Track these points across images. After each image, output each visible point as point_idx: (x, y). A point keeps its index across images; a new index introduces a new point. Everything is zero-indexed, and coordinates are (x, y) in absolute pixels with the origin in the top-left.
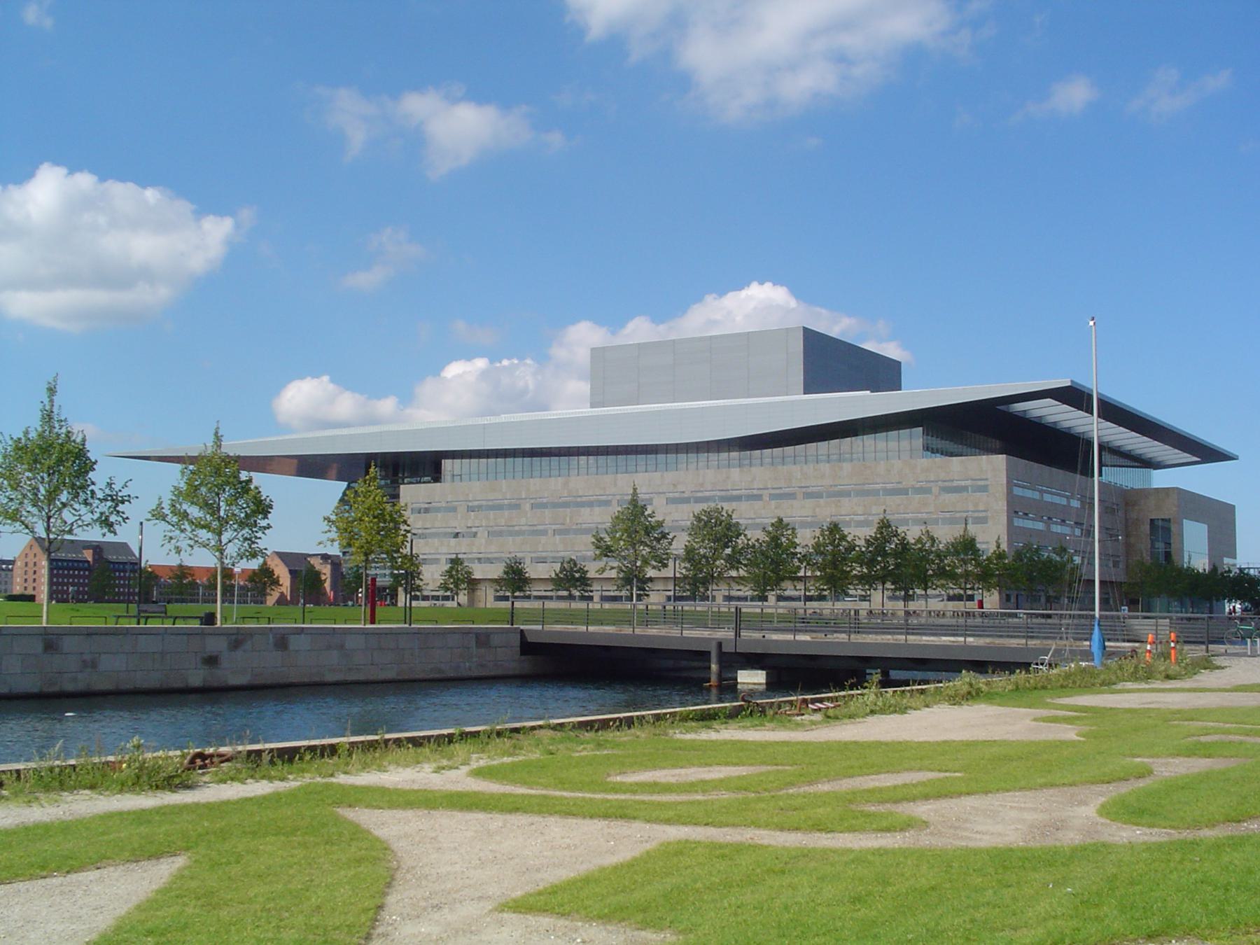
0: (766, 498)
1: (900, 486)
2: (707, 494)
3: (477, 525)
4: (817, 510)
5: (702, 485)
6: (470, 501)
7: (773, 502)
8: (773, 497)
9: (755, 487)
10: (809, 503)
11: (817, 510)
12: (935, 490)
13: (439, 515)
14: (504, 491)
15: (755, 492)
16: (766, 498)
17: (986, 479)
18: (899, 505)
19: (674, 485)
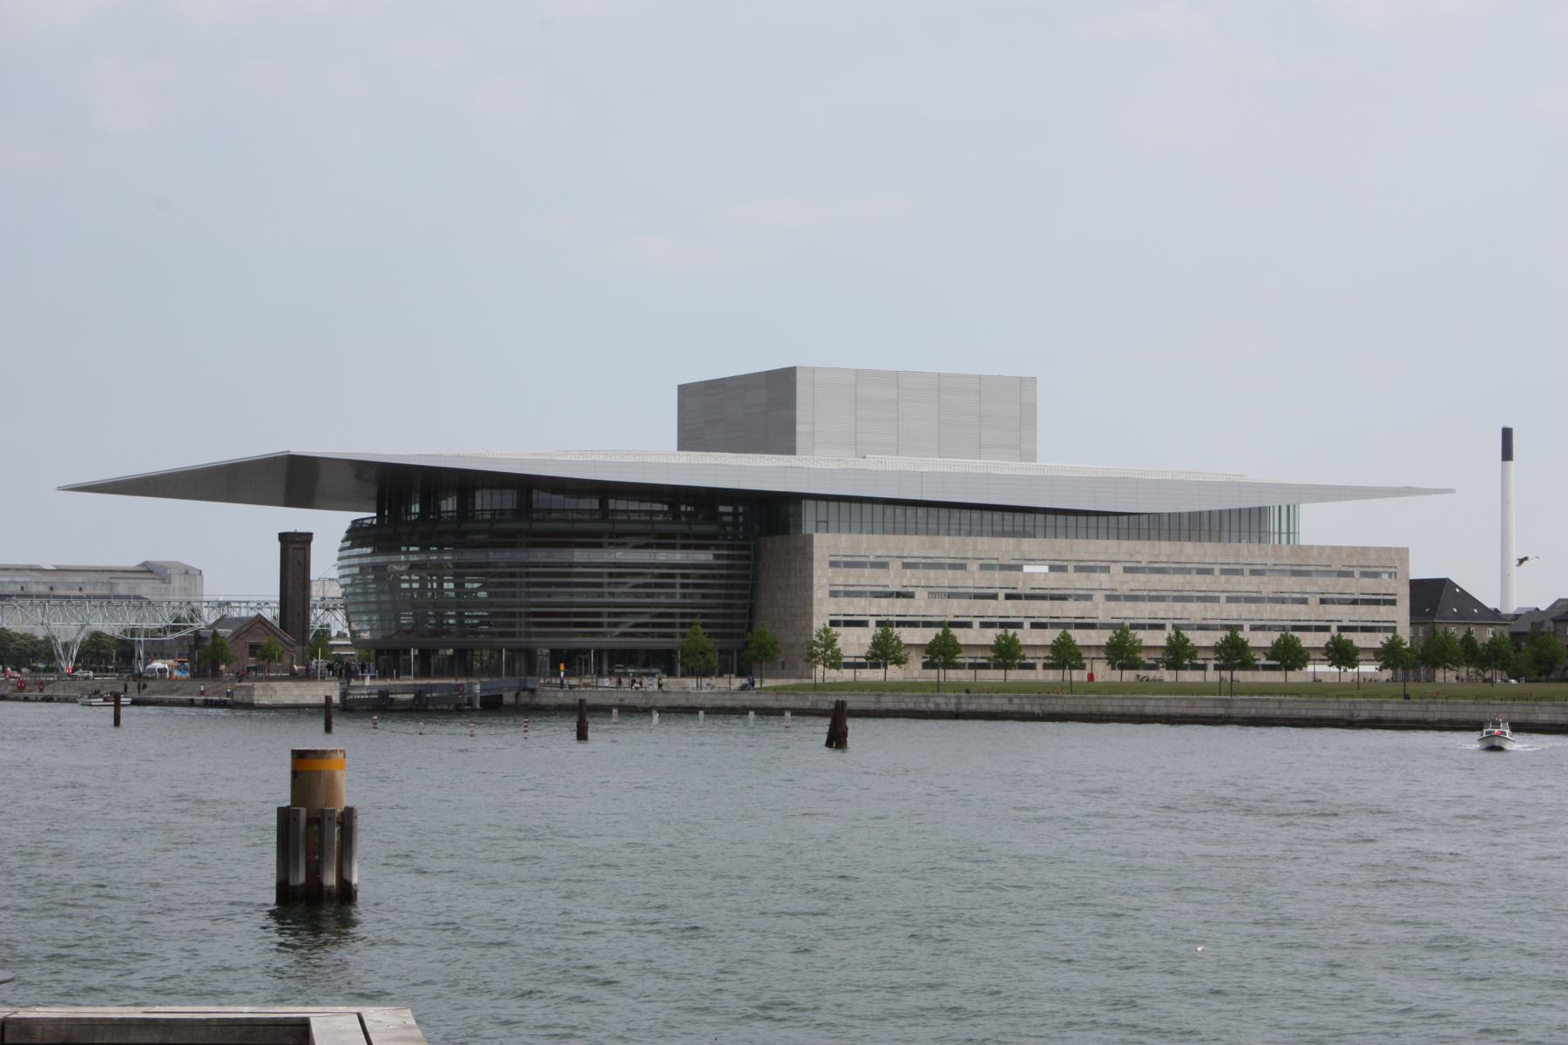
0: (1217, 572)
1: (1328, 569)
2: (1163, 565)
3: (914, 584)
4: (1262, 586)
5: (1157, 556)
6: (906, 557)
7: (1223, 578)
8: (1223, 572)
9: (1207, 561)
10: (1256, 579)
11: (1262, 586)
12: (1357, 574)
13: (867, 571)
14: (947, 548)
15: (1207, 566)
16: (1217, 572)
17: (1396, 567)
18: (1328, 586)
19: (1132, 555)
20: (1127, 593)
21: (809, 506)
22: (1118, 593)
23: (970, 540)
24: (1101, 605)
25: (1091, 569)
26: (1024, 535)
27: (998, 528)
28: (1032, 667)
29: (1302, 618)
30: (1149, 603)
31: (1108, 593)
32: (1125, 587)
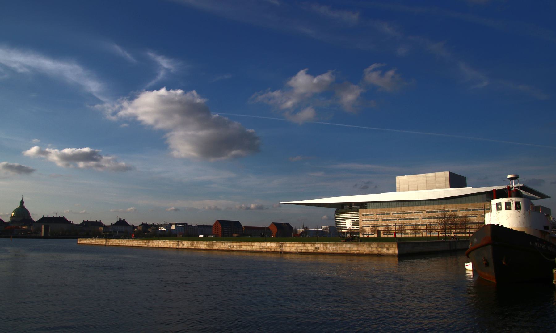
4: (463, 214)
5: (434, 208)
11: (463, 214)
20: (427, 217)
21: (368, 205)
22: (425, 217)
23: (390, 208)
24: (421, 220)
25: (419, 212)
26: (418, 206)
27: (412, 205)
28: (408, 234)
29: (476, 221)
30: (433, 219)
31: (423, 217)
32: (427, 216)
